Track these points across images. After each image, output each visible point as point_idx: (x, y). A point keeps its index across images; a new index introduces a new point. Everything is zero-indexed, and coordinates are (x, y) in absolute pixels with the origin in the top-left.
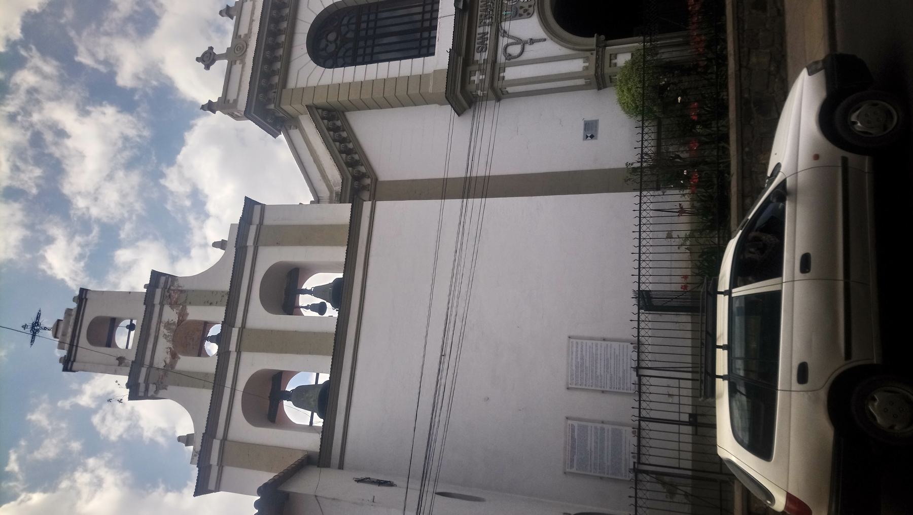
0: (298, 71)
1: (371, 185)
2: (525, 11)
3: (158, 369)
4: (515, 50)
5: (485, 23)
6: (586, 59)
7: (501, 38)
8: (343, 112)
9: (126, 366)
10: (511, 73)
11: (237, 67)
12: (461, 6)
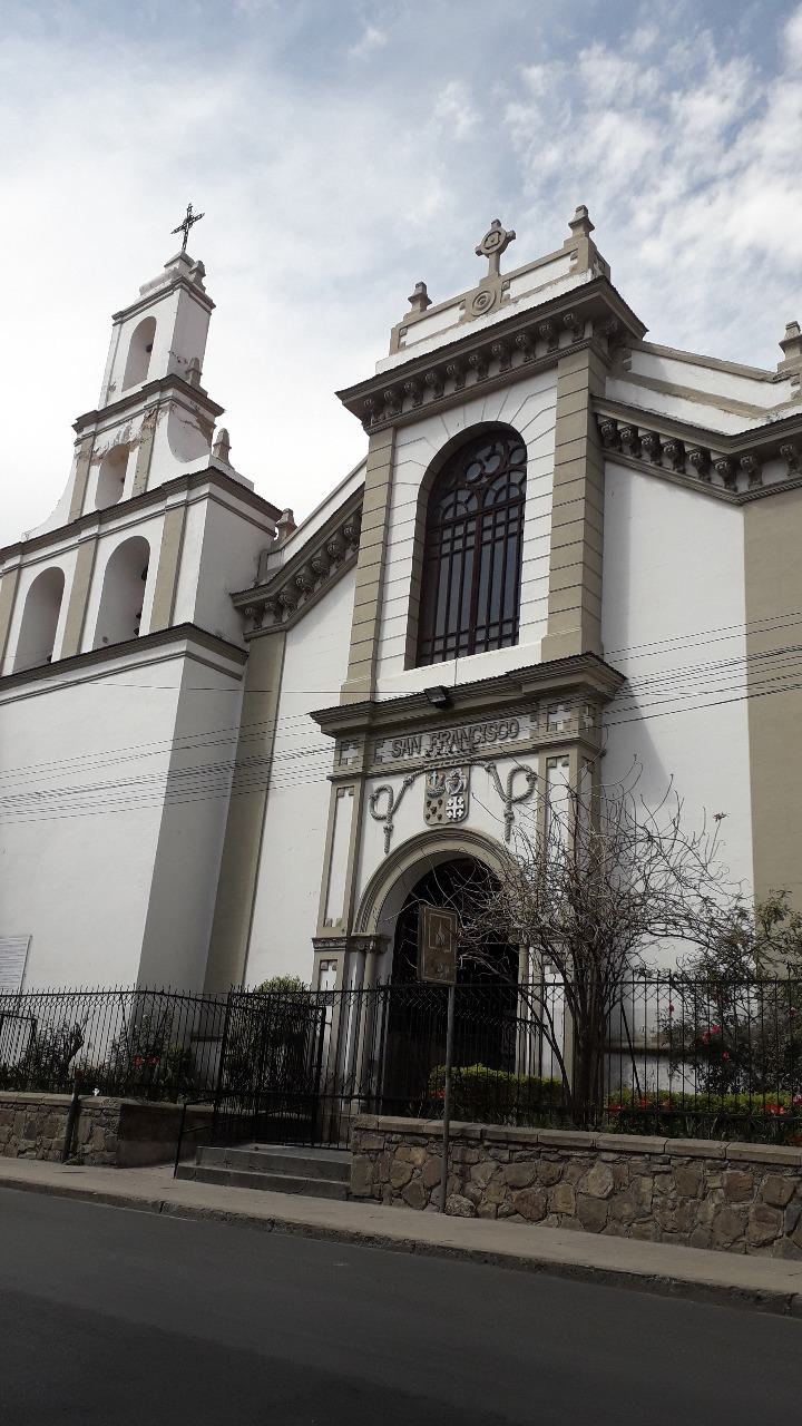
2: (434, 811)
3: (93, 445)
4: (382, 807)
9: (107, 400)
11: (456, 313)
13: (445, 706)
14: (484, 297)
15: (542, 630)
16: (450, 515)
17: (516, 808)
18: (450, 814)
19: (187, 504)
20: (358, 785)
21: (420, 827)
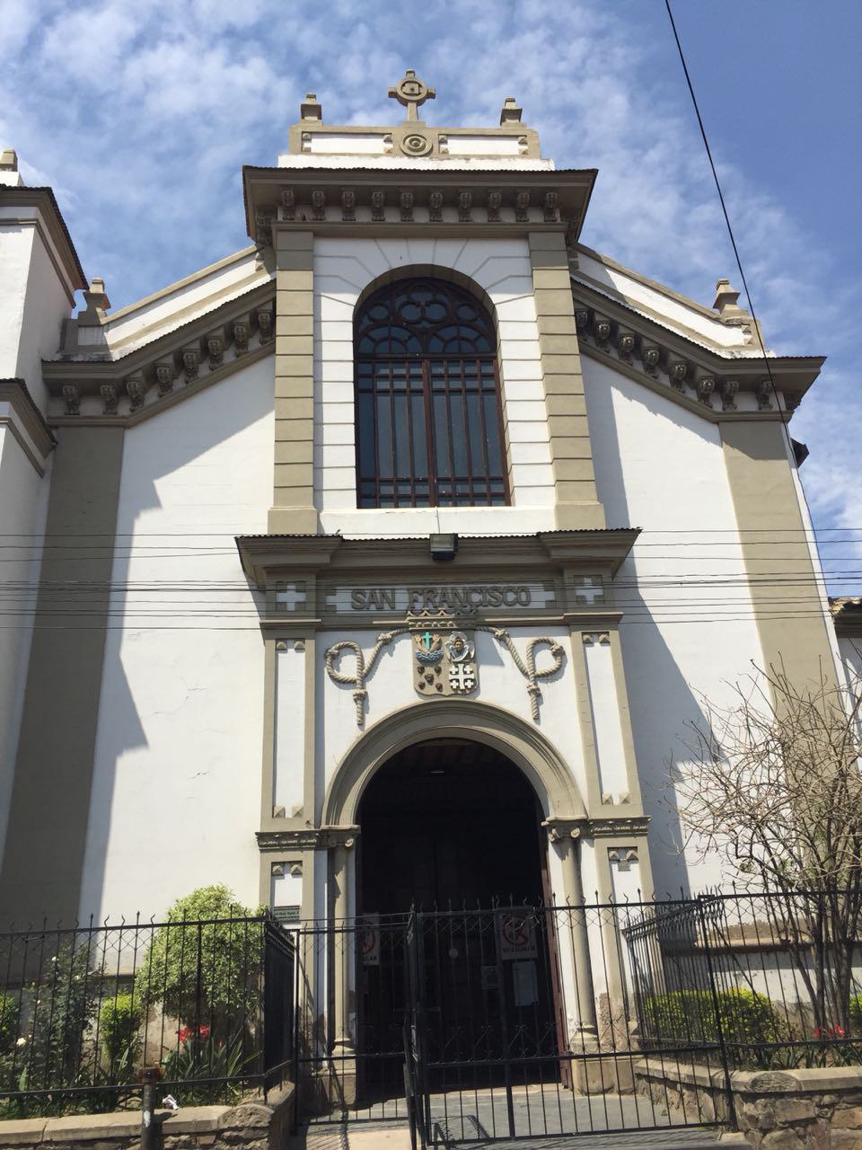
0: (353, 257)
1: (119, 418)
2: (430, 680)
4: (349, 667)
5: (415, 601)
6: (298, 814)
10: (295, 663)
11: (378, 145)
12: (436, 548)
14: (418, 140)
17: (540, 685)
18: (455, 684)
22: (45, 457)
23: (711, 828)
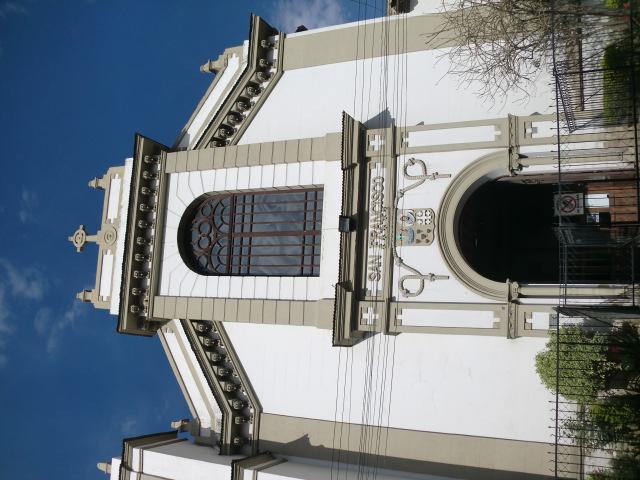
2: (424, 236)
4: (413, 285)
6: (497, 314)
7: (396, 267)
8: (220, 322)
13: (354, 223)
15: (320, 164)
16: (224, 260)
17: (430, 173)
18: (428, 222)
19: (141, 473)
20: (393, 306)
21: (435, 246)
22: (274, 458)
23: (513, 76)
